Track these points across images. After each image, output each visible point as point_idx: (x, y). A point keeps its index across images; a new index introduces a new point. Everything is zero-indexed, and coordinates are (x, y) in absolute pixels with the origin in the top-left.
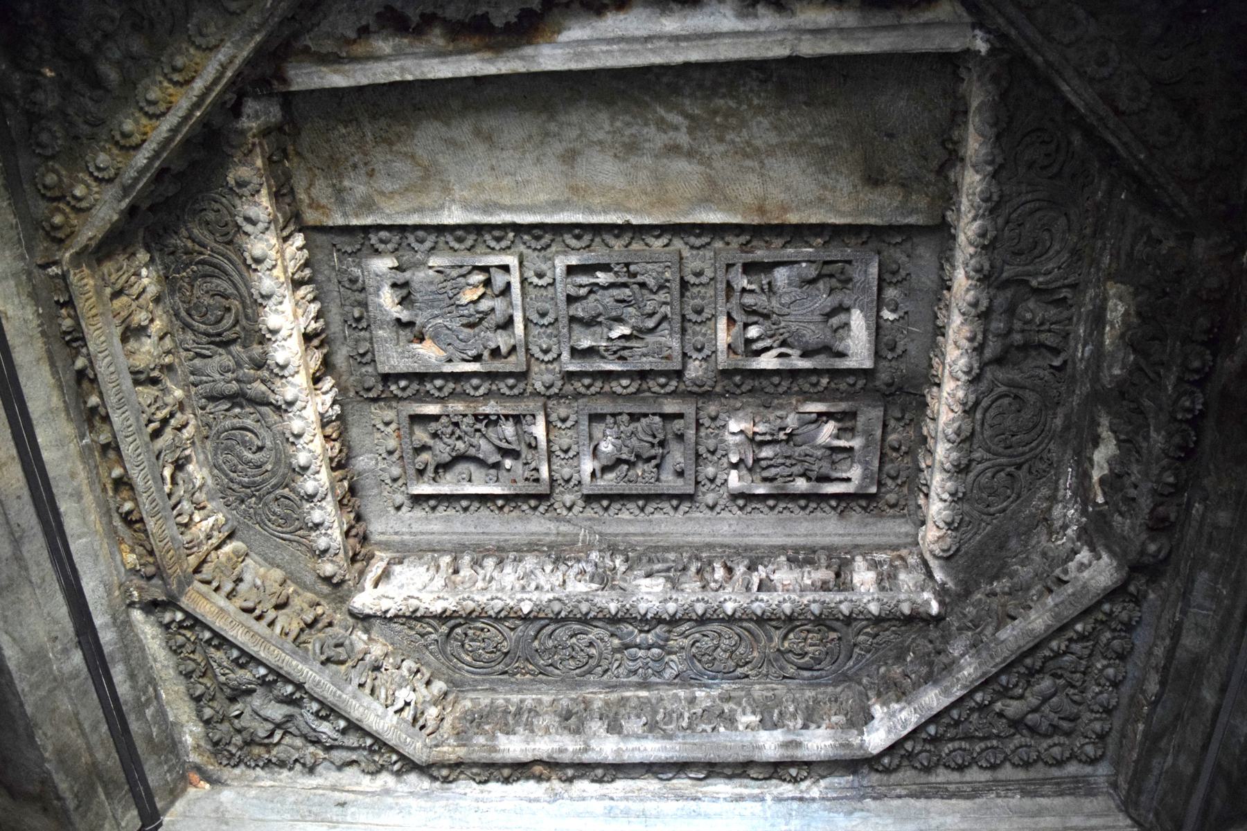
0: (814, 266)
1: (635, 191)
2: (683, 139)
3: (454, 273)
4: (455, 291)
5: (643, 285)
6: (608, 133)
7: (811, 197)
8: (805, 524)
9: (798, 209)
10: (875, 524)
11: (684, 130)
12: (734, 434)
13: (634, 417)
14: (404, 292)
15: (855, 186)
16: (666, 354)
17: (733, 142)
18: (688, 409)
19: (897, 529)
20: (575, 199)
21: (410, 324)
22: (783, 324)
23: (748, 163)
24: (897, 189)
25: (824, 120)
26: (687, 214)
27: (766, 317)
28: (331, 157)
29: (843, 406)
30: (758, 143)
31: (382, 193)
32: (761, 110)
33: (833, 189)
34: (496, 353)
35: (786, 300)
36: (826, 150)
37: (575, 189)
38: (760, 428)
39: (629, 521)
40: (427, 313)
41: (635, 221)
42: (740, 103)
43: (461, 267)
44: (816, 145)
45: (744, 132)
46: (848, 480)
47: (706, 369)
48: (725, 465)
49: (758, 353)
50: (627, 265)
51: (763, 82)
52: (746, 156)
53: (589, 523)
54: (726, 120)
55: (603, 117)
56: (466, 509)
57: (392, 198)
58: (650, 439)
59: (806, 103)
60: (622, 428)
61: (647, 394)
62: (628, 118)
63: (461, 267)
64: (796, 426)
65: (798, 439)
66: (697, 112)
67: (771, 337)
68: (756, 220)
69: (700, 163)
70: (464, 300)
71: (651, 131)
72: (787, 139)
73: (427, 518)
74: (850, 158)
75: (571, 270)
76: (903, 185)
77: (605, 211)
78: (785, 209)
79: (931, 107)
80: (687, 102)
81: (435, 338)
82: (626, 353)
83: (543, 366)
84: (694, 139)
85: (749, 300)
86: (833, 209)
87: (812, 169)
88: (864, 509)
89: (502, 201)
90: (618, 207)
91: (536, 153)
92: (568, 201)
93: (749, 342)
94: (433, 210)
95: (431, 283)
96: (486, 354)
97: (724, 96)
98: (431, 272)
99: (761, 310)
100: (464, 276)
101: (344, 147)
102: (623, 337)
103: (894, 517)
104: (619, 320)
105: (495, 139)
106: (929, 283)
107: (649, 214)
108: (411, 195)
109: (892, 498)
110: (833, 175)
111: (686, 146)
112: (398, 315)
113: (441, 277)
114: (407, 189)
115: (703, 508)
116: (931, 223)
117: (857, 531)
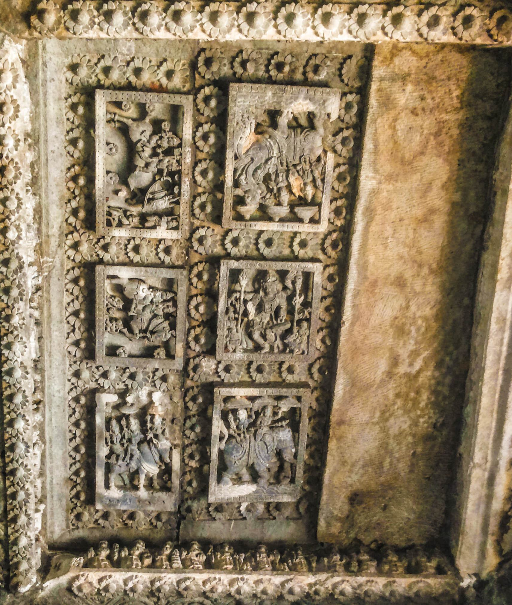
0: (292, 457)
1: (367, 331)
2: (402, 369)
3: (317, 174)
4: (301, 173)
5: (289, 332)
6: (414, 314)
7: (347, 456)
8: (60, 452)
9: (338, 448)
10: (61, 506)
11: (408, 370)
12: (150, 395)
13: (171, 318)
14: (303, 121)
15: (351, 486)
16: (230, 348)
17: (394, 404)
18: (178, 363)
19: (57, 524)
20: (367, 284)
21: (274, 125)
22: (247, 436)
23: (378, 414)
24: (346, 513)
25: (401, 465)
26: (344, 368)
27: (253, 424)
28: (434, 78)
29: (176, 481)
30: (392, 421)
31: (395, 120)
32: (415, 423)
33: (351, 471)
34: (240, 201)
35: (268, 438)
36: (381, 465)
37: (374, 284)
38: (158, 421)
39: (61, 302)
40: (283, 143)
41: (344, 330)
42: (422, 410)
43: (323, 180)
44: (384, 459)
45: (401, 412)
46: (107, 486)
47: (209, 375)
48: (117, 387)
49: (224, 416)
50: (308, 320)
51: (435, 426)
52: (383, 413)
53: (58, 265)
54: (411, 400)
55: (428, 311)
56: (73, 142)
57: (390, 127)
58: (151, 328)
59: (414, 454)
60: (161, 306)
61: (187, 325)
62: (423, 329)
63: (323, 180)
64: (159, 447)
65: (145, 447)
66: (420, 379)
67: (238, 427)
68: (334, 418)
69: (382, 381)
70: (292, 179)
71: (411, 346)
72: (391, 441)
73: (60, 99)
74: (372, 482)
75: (307, 276)
76: (348, 517)
77: (355, 306)
78: (340, 439)
79: (401, 532)
80: (429, 373)
81: (257, 145)
82: (231, 314)
83: (219, 237)
84: (400, 377)
85: (269, 412)
86: (336, 471)
87: (367, 457)
88: (77, 496)
89: (374, 224)
90: (356, 318)
91: (406, 255)
92: (366, 278)
93: (235, 412)
94: (375, 162)
95: (312, 150)
96: (239, 192)
97: (429, 399)
98: (319, 152)
99: (260, 420)
100: (314, 181)
101: (441, 92)
102: (246, 313)
103: (67, 520)
104: (260, 308)
105: (424, 225)
106: (269, 533)
107: (347, 341)
108: (391, 145)
109: (86, 516)
110: (361, 471)
111: (396, 371)
112: (285, 112)
113: (314, 158)
114: (395, 143)
115: (75, 367)
116: (319, 535)
117: (55, 493)
